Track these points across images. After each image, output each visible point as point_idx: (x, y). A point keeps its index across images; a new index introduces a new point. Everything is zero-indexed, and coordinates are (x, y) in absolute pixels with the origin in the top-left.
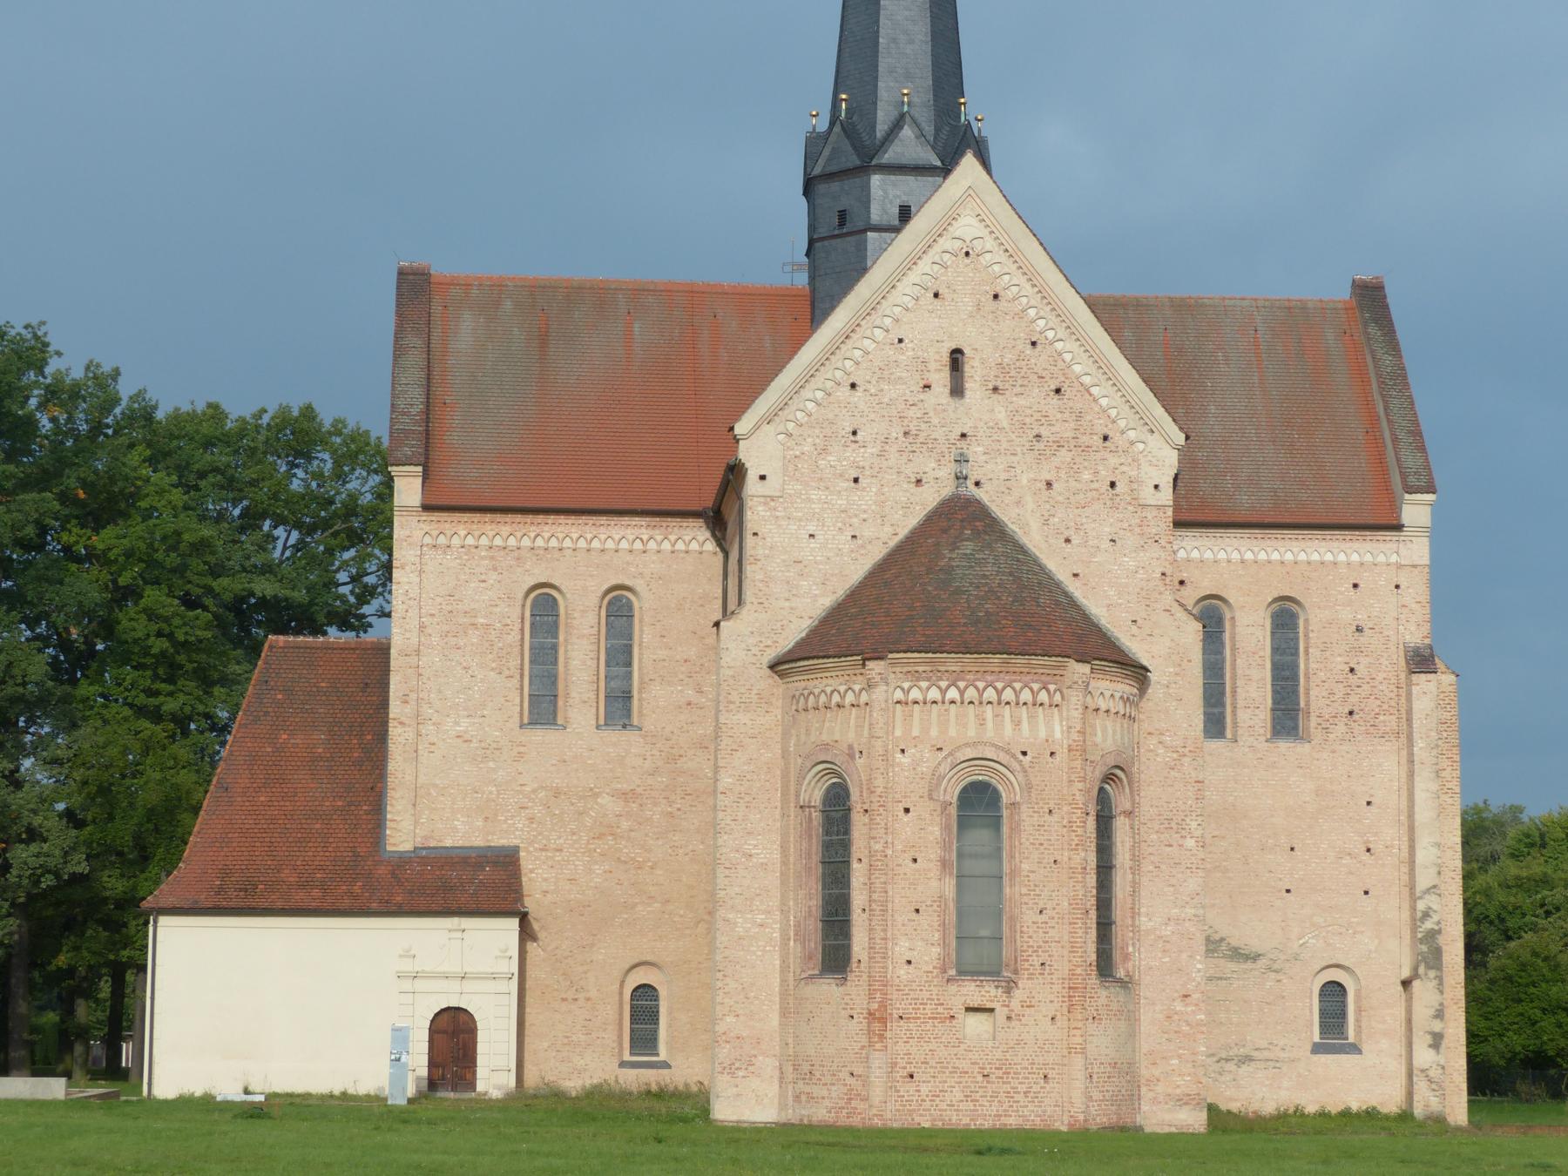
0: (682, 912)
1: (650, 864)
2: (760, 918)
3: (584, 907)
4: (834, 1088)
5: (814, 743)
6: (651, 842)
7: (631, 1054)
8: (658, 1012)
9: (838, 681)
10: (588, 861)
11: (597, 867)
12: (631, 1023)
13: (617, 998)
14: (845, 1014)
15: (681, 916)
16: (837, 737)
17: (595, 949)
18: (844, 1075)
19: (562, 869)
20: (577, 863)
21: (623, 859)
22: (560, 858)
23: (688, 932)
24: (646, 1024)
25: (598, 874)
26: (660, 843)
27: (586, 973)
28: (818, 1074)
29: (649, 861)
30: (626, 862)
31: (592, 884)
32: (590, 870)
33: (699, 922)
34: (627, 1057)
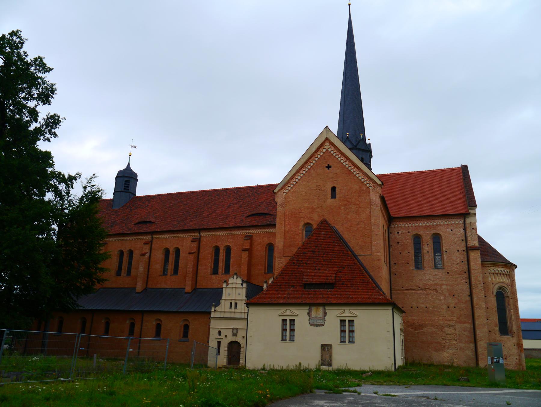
4: (513, 362)
5: (498, 281)
9: (502, 268)
14: (514, 344)
16: (505, 281)
18: (515, 359)
28: (509, 359)
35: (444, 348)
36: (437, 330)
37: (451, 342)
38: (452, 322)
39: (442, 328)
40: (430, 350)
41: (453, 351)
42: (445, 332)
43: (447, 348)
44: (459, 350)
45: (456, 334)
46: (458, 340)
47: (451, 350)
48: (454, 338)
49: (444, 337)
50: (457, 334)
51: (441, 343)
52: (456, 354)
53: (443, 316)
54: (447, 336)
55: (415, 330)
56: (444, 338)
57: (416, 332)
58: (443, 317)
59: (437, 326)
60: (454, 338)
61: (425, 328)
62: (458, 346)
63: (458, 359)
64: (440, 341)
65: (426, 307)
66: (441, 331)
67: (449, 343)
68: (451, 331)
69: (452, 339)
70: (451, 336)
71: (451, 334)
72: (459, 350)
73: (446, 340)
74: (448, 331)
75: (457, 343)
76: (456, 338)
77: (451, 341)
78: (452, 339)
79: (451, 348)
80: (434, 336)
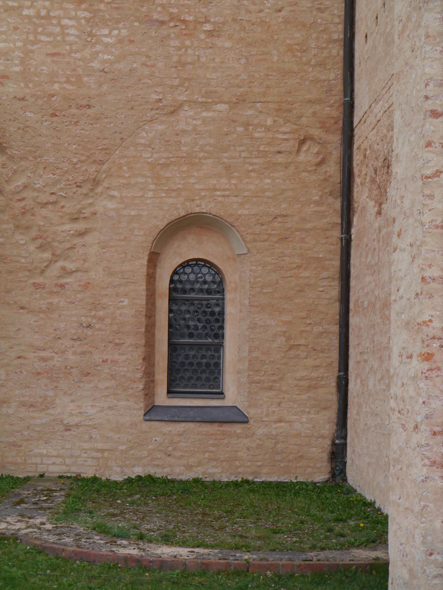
0: (269, 122)
1: (208, 27)
3: (79, 107)
8: (222, 313)
10: (88, 20)
11: (106, 31)
13: (142, 288)
15: (268, 129)
17: (99, 189)
19: (36, 33)
20: (66, 22)
21: (156, 16)
22: (32, 12)
23: (280, 159)
24: (199, 336)
25: (107, 45)
27: (82, 234)
29: (207, 21)
30: (162, 23)
31: (96, 65)
32: (90, 34)
33: (302, 142)
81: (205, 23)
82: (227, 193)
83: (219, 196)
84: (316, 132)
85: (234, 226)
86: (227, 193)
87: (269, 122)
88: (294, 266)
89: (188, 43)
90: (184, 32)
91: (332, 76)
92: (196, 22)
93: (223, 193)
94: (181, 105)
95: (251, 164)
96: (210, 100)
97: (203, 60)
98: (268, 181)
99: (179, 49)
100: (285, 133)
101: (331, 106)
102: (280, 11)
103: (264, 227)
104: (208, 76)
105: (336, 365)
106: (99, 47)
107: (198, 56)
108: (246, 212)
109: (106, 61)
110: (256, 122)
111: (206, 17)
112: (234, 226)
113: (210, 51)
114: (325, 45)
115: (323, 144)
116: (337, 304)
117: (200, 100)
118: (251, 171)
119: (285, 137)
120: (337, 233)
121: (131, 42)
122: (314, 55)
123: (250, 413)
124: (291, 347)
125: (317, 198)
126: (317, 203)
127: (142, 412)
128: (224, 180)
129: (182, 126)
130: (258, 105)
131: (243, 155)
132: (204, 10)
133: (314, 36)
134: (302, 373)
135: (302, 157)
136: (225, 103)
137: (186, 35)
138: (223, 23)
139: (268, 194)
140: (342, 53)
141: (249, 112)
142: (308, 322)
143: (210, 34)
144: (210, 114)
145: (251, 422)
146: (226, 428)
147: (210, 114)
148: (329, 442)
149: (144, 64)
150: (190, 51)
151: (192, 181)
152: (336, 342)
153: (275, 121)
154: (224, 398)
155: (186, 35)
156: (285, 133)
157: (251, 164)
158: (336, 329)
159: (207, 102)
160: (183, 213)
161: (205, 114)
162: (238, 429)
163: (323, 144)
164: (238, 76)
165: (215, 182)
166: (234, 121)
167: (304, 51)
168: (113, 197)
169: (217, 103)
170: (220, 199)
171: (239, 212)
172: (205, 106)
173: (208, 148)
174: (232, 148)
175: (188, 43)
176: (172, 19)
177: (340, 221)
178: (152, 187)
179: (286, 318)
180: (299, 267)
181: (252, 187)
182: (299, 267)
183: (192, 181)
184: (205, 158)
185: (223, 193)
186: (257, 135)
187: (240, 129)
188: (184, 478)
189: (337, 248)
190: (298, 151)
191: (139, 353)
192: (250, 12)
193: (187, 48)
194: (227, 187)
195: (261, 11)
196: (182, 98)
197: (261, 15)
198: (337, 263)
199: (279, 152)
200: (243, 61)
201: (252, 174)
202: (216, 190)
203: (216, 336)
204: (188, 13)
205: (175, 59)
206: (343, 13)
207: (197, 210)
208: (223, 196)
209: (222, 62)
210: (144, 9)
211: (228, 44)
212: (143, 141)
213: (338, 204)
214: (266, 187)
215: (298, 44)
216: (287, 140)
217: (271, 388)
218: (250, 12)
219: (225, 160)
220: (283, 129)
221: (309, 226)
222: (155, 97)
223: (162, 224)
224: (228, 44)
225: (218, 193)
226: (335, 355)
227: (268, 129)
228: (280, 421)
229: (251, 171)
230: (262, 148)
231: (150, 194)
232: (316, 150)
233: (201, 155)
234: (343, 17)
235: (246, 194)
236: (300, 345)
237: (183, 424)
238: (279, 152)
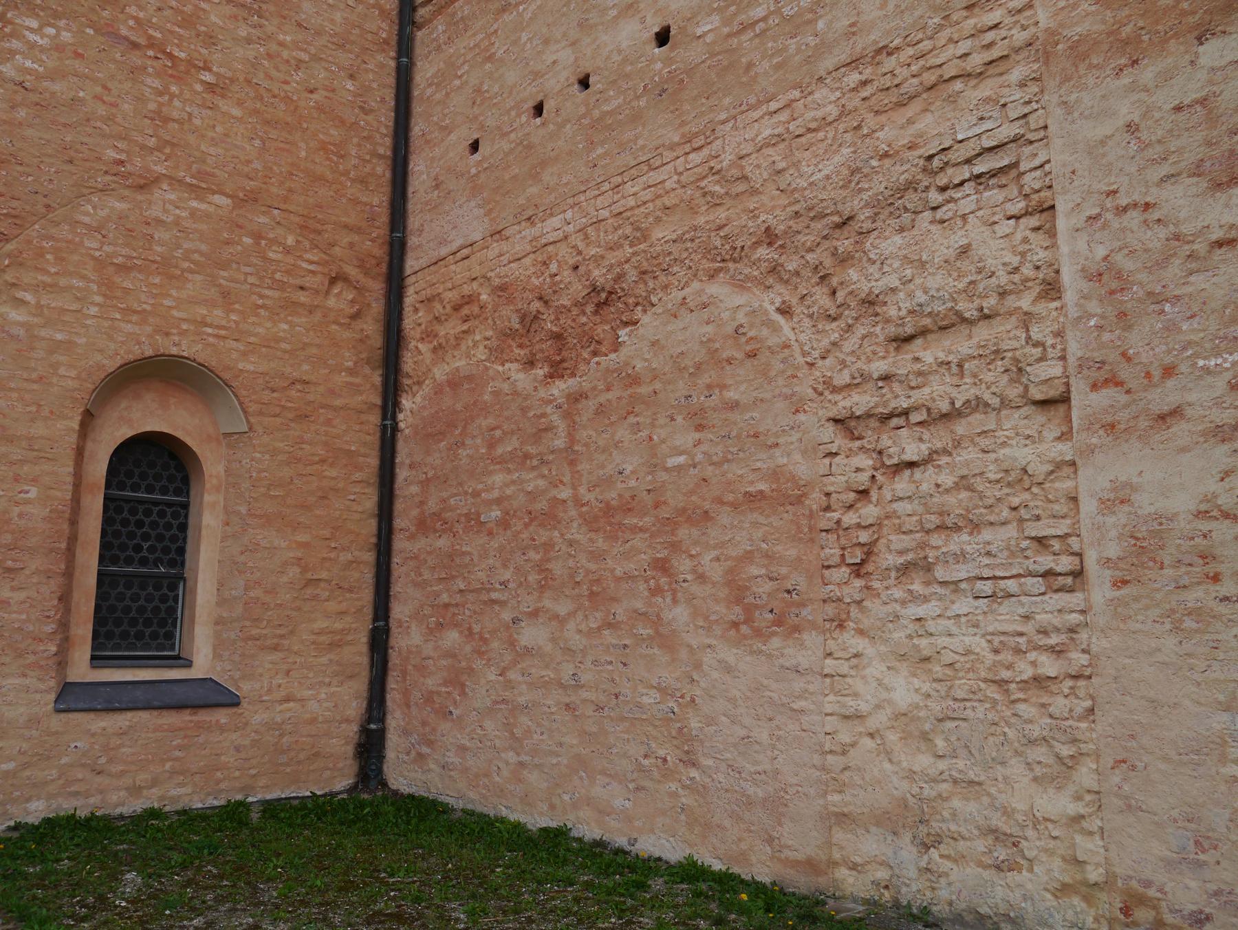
0: (290, 240)
1: (208, 77)
2: (554, 267)
6: (213, 18)
7: (97, 660)
11: (34, 24)
12: (102, 559)
13: (66, 470)
15: (287, 251)
23: (303, 297)
24: (144, 562)
25: (32, 46)
26: (243, 32)
30: (135, 46)
33: (333, 281)
34: (81, 669)
35: (858, 570)
36: (769, 301)
37: (968, 455)
38: (975, 93)
39: (844, 244)
40: (679, 614)
41: (1006, 617)
42: (870, 302)
43: (905, 570)
44: (1100, 591)
45: (1052, 289)
46: (1084, 401)
47: (963, 605)
48: (1018, 371)
49: (861, 381)
50: (1068, 277)
51: (815, 499)
52: (1049, 666)
53: (853, 63)
54: (902, 363)
55: (557, 370)
56: (861, 401)
57: (559, 388)
58: (854, 78)
59: (770, 236)
60: (1018, 371)
61: (646, 319)
62: (1088, 506)
63: (1085, 775)
64: (803, 468)
65: (663, 38)
66: (821, 298)
67: (926, 478)
68: (964, 251)
69: (978, 405)
70: (961, 344)
71: (968, 308)
72: (1100, 591)
73: (886, 441)
74: (923, 264)
75: (1065, 450)
76: (1053, 369)
77: (961, 428)
78: (978, 405)
79: (961, 557)
80: (734, 406)
81: (204, 69)
82: (223, 332)
83: (209, 335)
84: (352, 271)
85: (229, 386)
86: (223, 332)
87: (290, 240)
88: (317, 459)
89: (174, 89)
90: (170, 72)
91: (376, 201)
92: (190, 62)
93: (216, 331)
94: (157, 180)
95: (261, 296)
96: (204, 185)
97: (197, 122)
98: (285, 327)
99: (161, 94)
100: (312, 262)
101: (373, 241)
102: (311, 92)
103: (275, 395)
104: (203, 148)
105: (368, 612)
106: (15, 44)
107: (190, 114)
108: (251, 367)
109: (29, 71)
110: (271, 236)
111: (205, 62)
112: (229, 386)
113: (209, 112)
114: (368, 157)
115: (360, 290)
116: (373, 524)
117: (188, 180)
118: (261, 307)
119: (311, 267)
120: (374, 418)
121: (78, 55)
122: (354, 166)
123: (245, 689)
124: (310, 582)
125: (350, 364)
126: (351, 372)
127: (53, 696)
128: (218, 312)
129: (156, 211)
130: (276, 212)
131: (251, 280)
132: (204, 51)
133: (355, 140)
134: (321, 624)
135: (331, 302)
136: (228, 196)
137: (172, 76)
138: (232, 80)
139: (284, 346)
140: (388, 174)
141: (262, 219)
142: (333, 545)
143: (210, 88)
144: (203, 206)
145: (244, 704)
146: (204, 716)
147: (203, 206)
148: (355, 728)
149: (97, 98)
150: (176, 103)
151: (167, 302)
152: (369, 576)
153: (298, 241)
154: (189, 664)
155: (172, 76)
156: (312, 262)
157: (261, 296)
158: (370, 557)
159: (199, 187)
160: (149, 352)
161: (194, 204)
162: (222, 716)
163: (360, 290)
164: (249, 162)
165: (205, 312)
166: (241, 227)
167: (342, 157)
168: (23, 302)
169: (214, 193)
170: (211, 340)
171: (240, 366)
172: (195, 191)
173: (196, 256)
174: (234, 266)
175: (174, 89)
176: (151, 46)
177: (379, 401)
178: (98, 299)
179: (302, 537)
180: (323, 461)
181: (261, 330)
182: (323, 461)
183: (167, 302)
184: (192, 272)
185: (216, 331)
186: (271, 255)
187: (248, 240)
188: (126, 810)
189: (374, 439)
190: (327, 293)
191: (51, 588)
192: (272, 79)
193: (172, 96)
194: (224, 323)
195: (286, 83)
196: (159, 169)
197: (286, 87)
198: (374, 461)
199: (302, 288)
200: (257, 143)
201: (262, 312)
202: (206, 325)
203: (172, 563)
204: (178, 46)
205: (152, 106)
206: (391, 124)
207: (174, 351)
208: (217, 336)
209: (226, 135)
210: (105, 14)
211: (236, 112)
212: (87, 220)
213: (377, 379)
214: (281, 334)
215: (335, 145)
216: (313, 272)
217: (276, 648)
218: (272, 79)
219: (222, 281)
220: (308, 256)
221: (338, 402)
222: (111, 154)
223: (112, 365)
224: (236, 112)
225: (210, 330)
226: (366, 596)
227: (287, 251)
228: (288, 699)
229: (261, 307)
230: (278, 276)
231: (94, 310)
232: (350, 297)
233: (186, 265)
234: (391, 129)
235: (252, 339)
236: (320, 580)
237: (129, 715)
238: (302, 288)
